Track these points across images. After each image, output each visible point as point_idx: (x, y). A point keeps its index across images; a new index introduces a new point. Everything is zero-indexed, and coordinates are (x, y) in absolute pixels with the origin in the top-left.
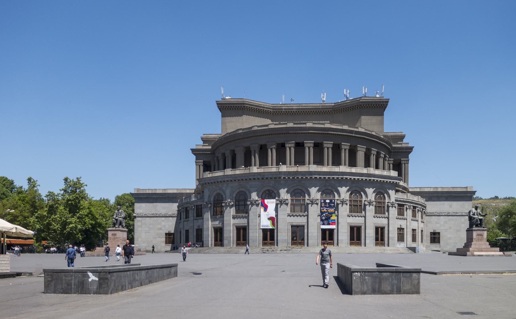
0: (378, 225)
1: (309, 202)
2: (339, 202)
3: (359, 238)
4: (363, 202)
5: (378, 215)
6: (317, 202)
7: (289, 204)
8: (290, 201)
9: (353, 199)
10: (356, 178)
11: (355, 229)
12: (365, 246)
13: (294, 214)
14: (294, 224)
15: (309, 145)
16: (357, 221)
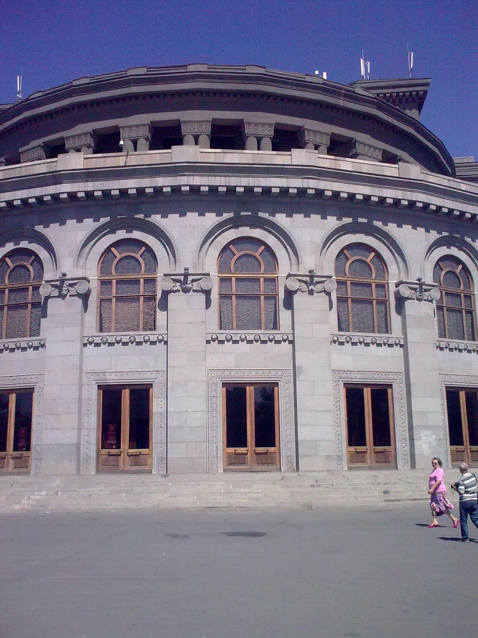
0: (456, 382)
1: (169, 285)
2: (293, 285)
3: (383, 436)
4: (392, 289)
5: (454, 343)
6: (204, 284)
7: (93, 300)
8: (94, 286)
9: (348, 278)
10: (361, 190)
11: (367, 394)
12: (413, 465)
13: (111, 336)
14: (112, 379)
15: (196, 129)
16: (371, 362)
